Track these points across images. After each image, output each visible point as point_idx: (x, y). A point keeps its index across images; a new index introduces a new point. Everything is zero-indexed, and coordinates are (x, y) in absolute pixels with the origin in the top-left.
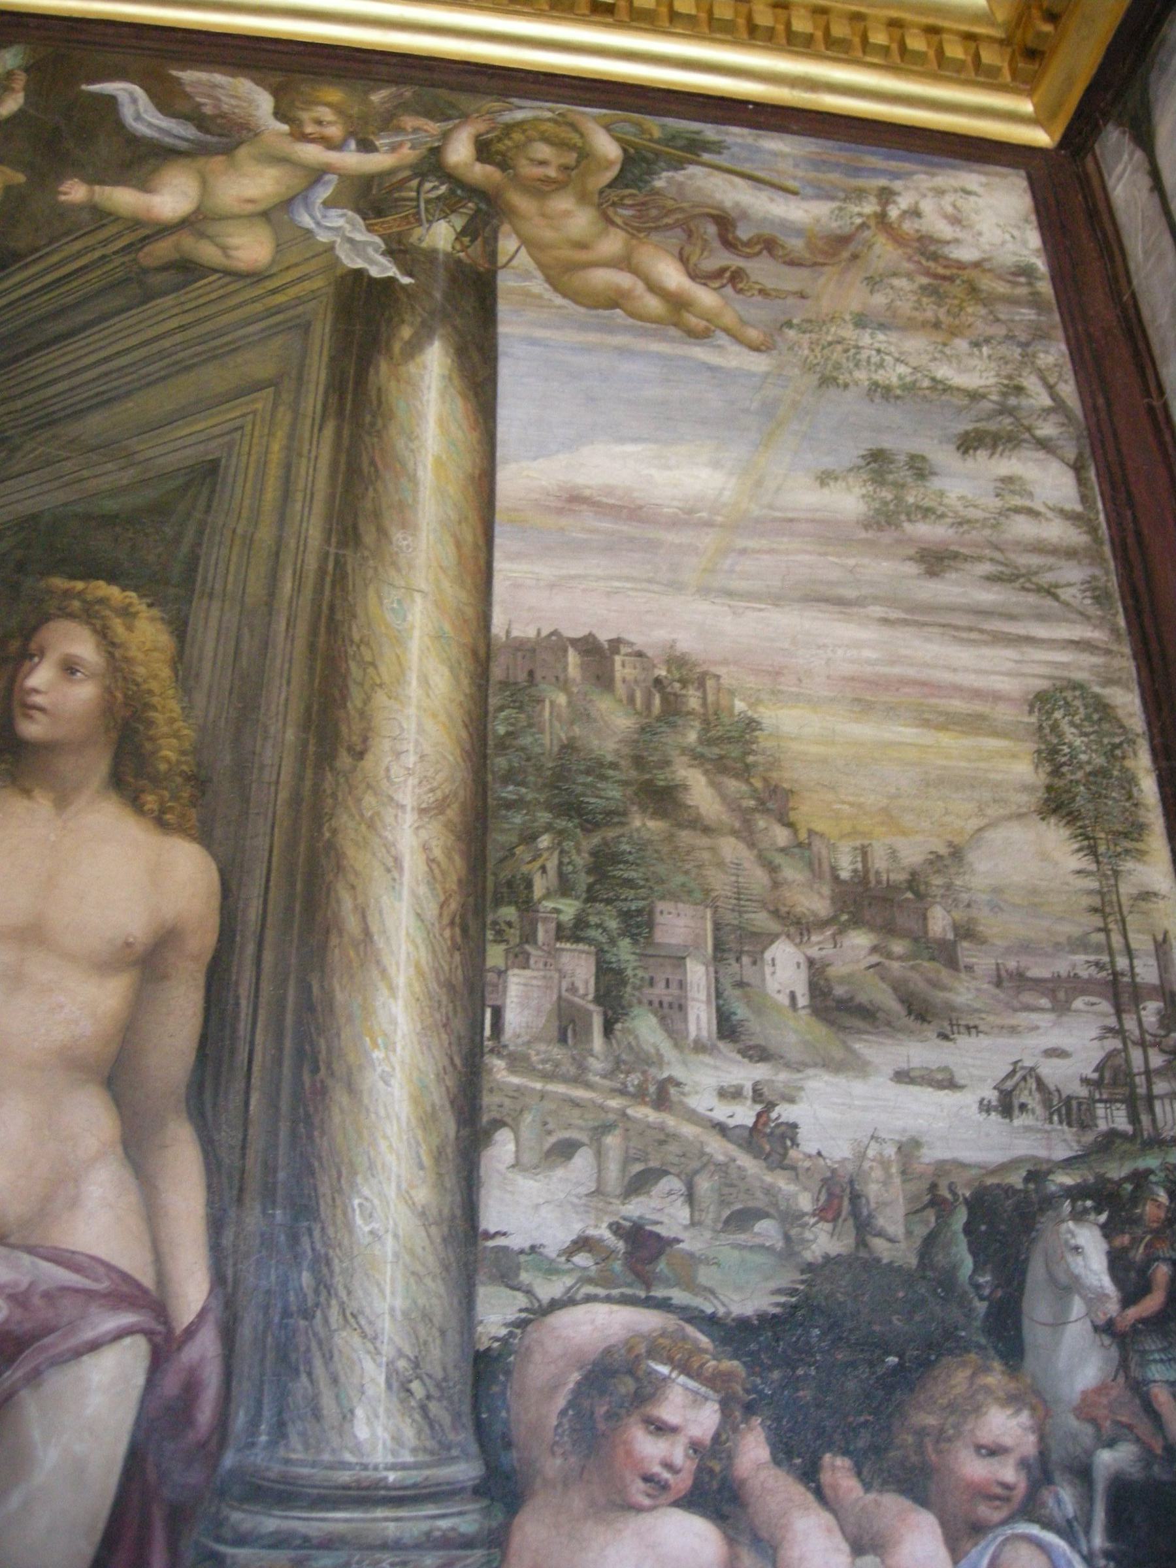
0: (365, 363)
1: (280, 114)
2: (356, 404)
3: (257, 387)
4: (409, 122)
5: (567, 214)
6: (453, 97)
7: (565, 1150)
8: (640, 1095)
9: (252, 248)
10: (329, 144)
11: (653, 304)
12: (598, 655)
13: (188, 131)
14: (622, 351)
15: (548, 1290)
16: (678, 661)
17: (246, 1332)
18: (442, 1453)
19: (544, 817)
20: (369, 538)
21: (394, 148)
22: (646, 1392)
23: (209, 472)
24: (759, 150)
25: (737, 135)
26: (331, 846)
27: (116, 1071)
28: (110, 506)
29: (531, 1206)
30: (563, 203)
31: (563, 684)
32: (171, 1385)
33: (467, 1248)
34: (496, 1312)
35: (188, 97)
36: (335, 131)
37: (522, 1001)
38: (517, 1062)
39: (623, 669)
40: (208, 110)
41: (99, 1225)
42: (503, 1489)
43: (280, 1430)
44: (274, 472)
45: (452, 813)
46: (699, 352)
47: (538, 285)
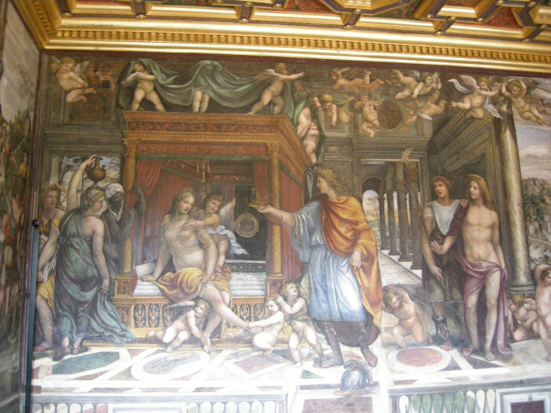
0: (499, 134)
1: (478, 85)
2: (500, 143)
3: (486, 140)
4: (496, 84)
5: (520, 101)
6: (502, 77)
7: (537, 247)
8: (544, 240)
9: (480, 113)
10: (487, 91)
11: (534, 119)
12: (534, 180)
13: (465, 89)
14: (531, 128)
15: (538, 263)
16: (543, 181)
17: (509, 269)
18: (529, 280)
19: (531, 205)
20: (505, 165)
21: (495, 90)
22: (548, 274)
23: (483, 155)
24: (545, 83)
25: (541, 80)
26: (509, 211)
27: (491, 240)
28: (474, 162)
29: (535, 254)
30: (520, 99)
31: (531, 185)
32: (503, 275)
33: (529, 260)
34: (533, 266)
35: (463, 81)
36: (486, 87)
37: (531, 229)
38: (532, 237)
39: (537, 183)
40: (467, 84)
41: (493, 258)
42: (535, 284)
43: (514, 280)
44: (492, 154)
45: (521, 205)
46: (541, 127)
47: (519, 117)
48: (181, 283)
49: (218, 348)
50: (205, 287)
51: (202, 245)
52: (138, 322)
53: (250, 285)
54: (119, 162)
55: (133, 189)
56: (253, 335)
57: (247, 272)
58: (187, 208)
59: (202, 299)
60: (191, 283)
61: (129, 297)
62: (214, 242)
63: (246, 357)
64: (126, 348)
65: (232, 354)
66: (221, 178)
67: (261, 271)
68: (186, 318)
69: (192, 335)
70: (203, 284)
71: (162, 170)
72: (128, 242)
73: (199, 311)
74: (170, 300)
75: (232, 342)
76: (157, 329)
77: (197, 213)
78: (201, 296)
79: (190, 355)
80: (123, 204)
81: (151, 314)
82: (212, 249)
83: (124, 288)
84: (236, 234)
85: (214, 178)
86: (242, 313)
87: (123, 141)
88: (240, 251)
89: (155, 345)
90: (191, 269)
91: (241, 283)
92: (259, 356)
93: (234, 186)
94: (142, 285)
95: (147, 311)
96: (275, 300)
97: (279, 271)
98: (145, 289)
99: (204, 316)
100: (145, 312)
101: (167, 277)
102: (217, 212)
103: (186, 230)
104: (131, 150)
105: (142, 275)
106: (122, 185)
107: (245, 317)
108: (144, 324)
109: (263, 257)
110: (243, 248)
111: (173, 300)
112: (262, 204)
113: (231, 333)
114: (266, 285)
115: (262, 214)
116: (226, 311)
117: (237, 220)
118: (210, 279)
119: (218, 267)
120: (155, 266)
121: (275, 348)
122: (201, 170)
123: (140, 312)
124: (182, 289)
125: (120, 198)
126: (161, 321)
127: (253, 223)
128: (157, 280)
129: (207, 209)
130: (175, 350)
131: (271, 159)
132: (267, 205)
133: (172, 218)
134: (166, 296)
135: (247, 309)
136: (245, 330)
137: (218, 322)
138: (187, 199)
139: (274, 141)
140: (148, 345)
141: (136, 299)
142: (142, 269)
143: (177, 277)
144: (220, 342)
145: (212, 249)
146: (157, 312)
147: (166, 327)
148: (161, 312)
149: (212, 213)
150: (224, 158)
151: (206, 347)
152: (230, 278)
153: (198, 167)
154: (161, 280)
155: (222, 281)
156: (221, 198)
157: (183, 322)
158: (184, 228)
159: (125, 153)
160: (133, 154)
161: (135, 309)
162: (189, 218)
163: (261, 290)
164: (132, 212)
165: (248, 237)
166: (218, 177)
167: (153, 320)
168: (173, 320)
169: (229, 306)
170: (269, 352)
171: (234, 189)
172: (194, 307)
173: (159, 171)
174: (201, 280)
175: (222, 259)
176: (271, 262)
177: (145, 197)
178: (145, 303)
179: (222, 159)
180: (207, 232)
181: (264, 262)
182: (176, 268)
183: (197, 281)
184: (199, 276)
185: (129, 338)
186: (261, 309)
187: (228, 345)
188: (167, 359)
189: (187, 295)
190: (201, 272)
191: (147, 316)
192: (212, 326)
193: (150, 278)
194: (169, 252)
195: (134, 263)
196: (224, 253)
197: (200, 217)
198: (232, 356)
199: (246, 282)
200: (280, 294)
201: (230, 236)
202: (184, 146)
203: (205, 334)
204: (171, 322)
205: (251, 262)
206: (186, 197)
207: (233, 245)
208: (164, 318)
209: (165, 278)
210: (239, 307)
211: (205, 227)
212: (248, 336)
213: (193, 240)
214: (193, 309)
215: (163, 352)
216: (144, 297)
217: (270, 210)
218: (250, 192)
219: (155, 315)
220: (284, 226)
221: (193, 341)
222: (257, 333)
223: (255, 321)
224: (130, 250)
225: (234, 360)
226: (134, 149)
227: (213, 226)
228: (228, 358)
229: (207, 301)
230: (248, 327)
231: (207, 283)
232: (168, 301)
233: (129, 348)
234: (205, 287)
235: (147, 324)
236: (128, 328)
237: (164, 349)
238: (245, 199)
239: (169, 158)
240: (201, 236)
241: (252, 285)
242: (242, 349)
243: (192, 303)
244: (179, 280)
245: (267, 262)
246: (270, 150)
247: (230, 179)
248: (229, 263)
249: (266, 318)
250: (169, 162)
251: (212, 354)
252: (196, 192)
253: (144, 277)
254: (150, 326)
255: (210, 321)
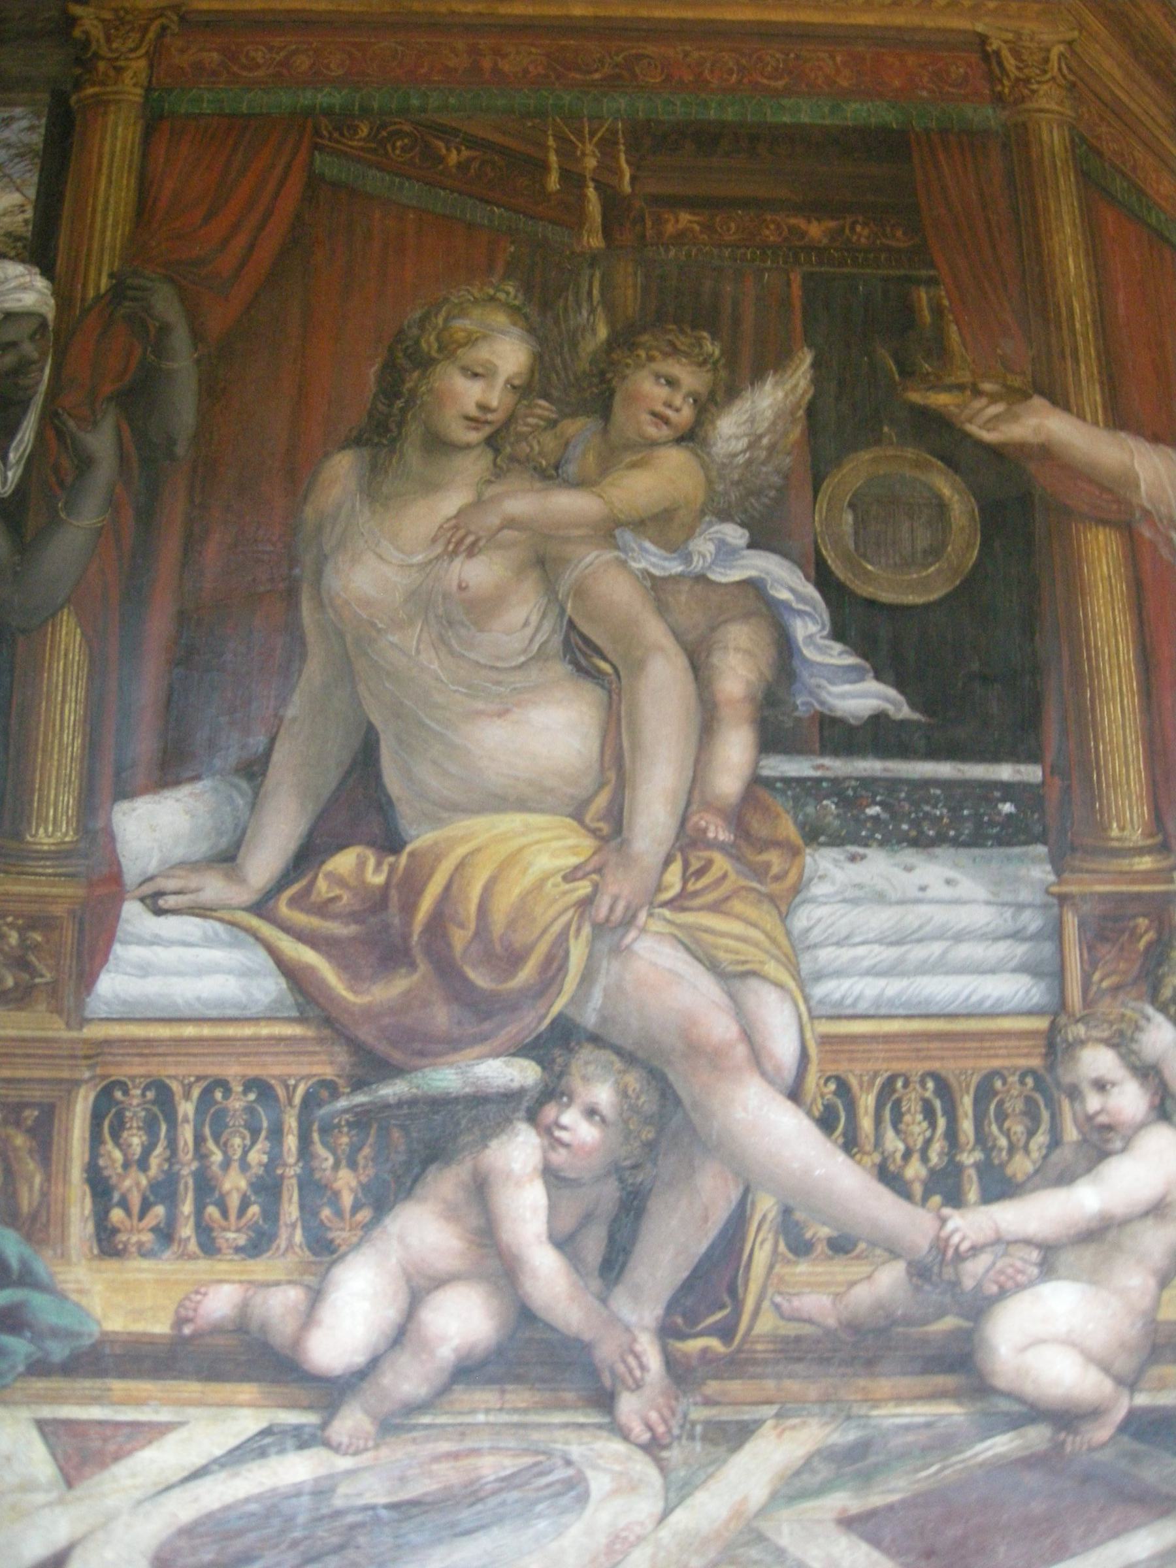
48: (439, 922)
49: (726, 1414)
50: (618, 951)
51: (588, 656)
52: (117, 1215)
53: (938, 936)
54: (36, 139)
55: (119, 290)
56: (980, 1307)
57: (918, 842)
58: (483, 407)
59: (596, 1040)
60: (512, 924)
61: (57, 1029)
62: (677, 635)
63: (929, 1474)
64: (25, 1413)
65: (828, 1454)
66: (708, 228)
67: (1011, 834)
68: (481, 1190)
69: (523, 1316)
70: (599, 929)
71: (314, 181)
72: (68, 638)
73: (579, 1129)
74: (356, 1047)
75: (824, 1361)
76: (259, 1268)
77: (549, 442)
78: (590, 1018)
79: (509, 1465)
80: (43, 388)
81: (217, 1157)
82: (663, 683)
83: (21, 964)
84: (823, 579)
85: (659, 221)
86: (893, 1143)
87: (73, 21)
88: (862, 696)
89: (247, 1391)
90: (512, 821)
91: (881, 919)
92: (1029, 1462)
93: (796, 279)
94: (155, 941)
95: (187, 1134)
96: (1122, 1042)
97: (1136, 836)
98: (178, 969)
99: (616, 1170)
100: (172, 1143)
101: (340, 882)
102: (691, 437)
103: (471, 552)
104: (119, 70)
105: (153, 867)
106: (48, 272)
107: (915, 1170)
108: (166, 1234)
109: (1020, 741)
110: (878, 677)
111: (382, 1048)
112: (987, 386)
113: (817, 1295)
114: (1057, 933)
115: (996, 452)
116: (776, 1130)
117: (827, 487)
118: (652, 898)
119: (707, 806)
120: (254, 805)
121: (1142, 1400)
122: (572, 179)
123: (136, 1141)
124: (447, 971)
125: (29, 349)
126: (291, 1210)
127: (941, 507)
128: (262, 907)
129: (619, 413)
130: (398, 1429)
131: (1024, 124)
132: (1027, 397)
133: (375, 471)
134: (328, 1021)
135: (929, 1113)
136: (920, 1272)
137: (720, 1215)
138: (483, 352)
139: (1029, 27)
140: (193, 1388)
141: (108, 1042)
142: (155, 827)
143: (410, 885)
144: (736, 1365)
145: (663, 683)
146: (262, 1144)
147: (325, 1251)
148: (291, 1142)
149: (653, 444)
150: (718, 111)
151: (628, 1406)
152: (797, 889)
153: (553, 158)
154: (293, 902)
155: (738, 906)
156: (712, 348)
157: (451, 1214)
158: (460, 540)
159: (78, 85)
160: (131, 88)
161: (97, 1117)
162: (498, 473)
163: (1026, 968)
164: (102, 441)
165: (910, 599)
166: (685, 217)
167: (234, 1202)
168: (382, 1199)
169: (795, 1095)
170: (1102, 1432)
171: (796, 290)
172: (533, 1106)
173: (296, 184)
174: (586, 903)
175: (736, 751)
176: (1079, 772)
177: (197, 336)
178: (173, 1071)
179: (712, 114)
180: (623, 564)
181: (1032, 773)
182: (406, 814)
183: (553, 912)
184: (571, 875)
185: (56, 1333)
186: (1031, 1114)
187: (793, 1386)
188: (338, 1502)
189: (487, 1016)
190: (588, 844)
191: (188, 1167)
192: (670, 1247)
193: (214, 888)
194: (356, 701)
195: (107, 782)
196: (746, 710)
197: (571, 469)
198: (825, 1471)
199: (913, 917)
200: (1154, 999)
201: (784, 595)
202: (460, 45)
203: (623, 1305)
204: (365, 1215)
205: (945, 770)
206: (471, 341)
207: (809, 653)
208: (314, 1189)
209: (322, 884)
210: (867, 1101)
211: (607, 531)
212: (941, 1314)
213: (522, 618)
214: (532, 1117)
215: (302, 1445)
216: (164, 1031)
217: (1044, 424)
218: (908, 310)
219: (244, 1166)
220: (1147, 533)
221: (535, 1359)
222: (1003, 1294)
223: (989, 1197)
224: (76, 693)
225: (842, 1500)
226: (143, 63)
227: (664, 524)
228: (793, 1488)
229: (629, 1058)
230: (940, 1245)
231: (628, 921)
232: (342, 1056)
233: (47, 1412)
234: (618, 951)
235: (186, 1231)
236: (41, 1266)
237: (309, 1419)
238: (874, 367)
239: (365, 111)
240: (580, 592)
241: (959, 937)
242: (904, 1412)
243: (521, 1073)
244: (426, 904)
245: (1052, 771)
246: (1013, 72)
247: (770, 235)
248: (788, 781)
249: (1065, 1178)
250: (364, 130)
251: (674, 1455)
252: (543, 303)
253: (171, 884)
254: (209, 1247)
255: (655, 1205)
